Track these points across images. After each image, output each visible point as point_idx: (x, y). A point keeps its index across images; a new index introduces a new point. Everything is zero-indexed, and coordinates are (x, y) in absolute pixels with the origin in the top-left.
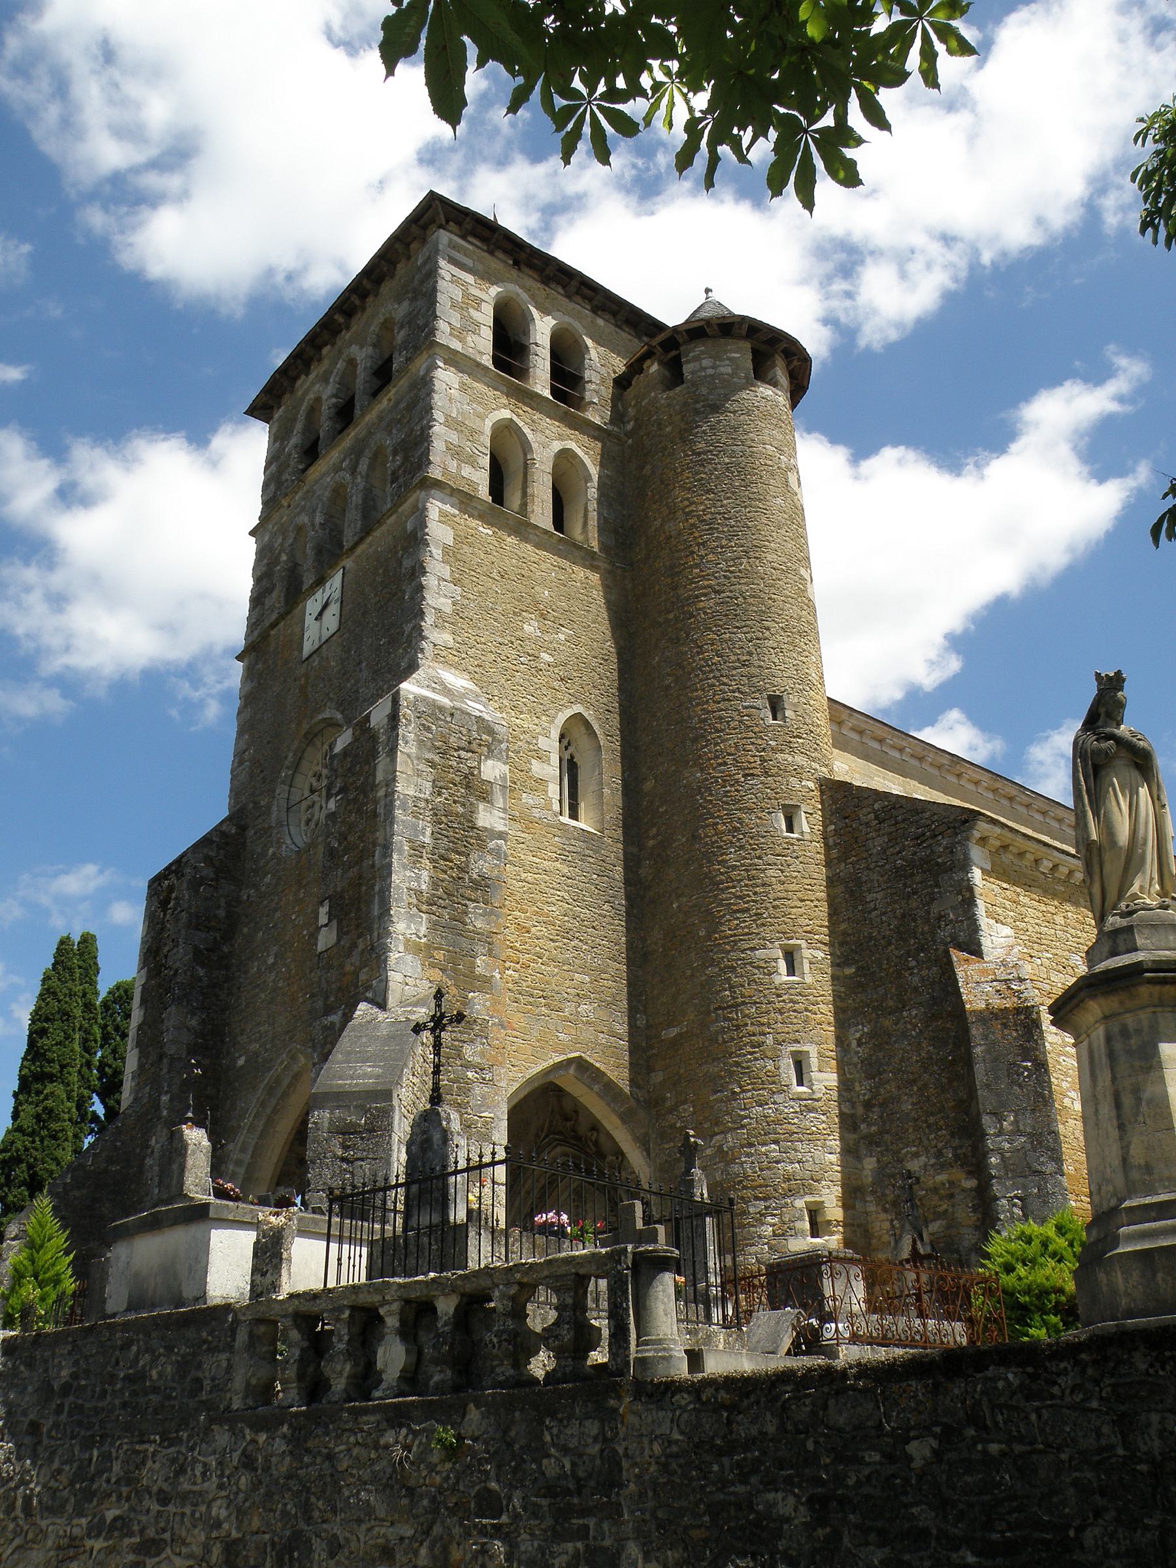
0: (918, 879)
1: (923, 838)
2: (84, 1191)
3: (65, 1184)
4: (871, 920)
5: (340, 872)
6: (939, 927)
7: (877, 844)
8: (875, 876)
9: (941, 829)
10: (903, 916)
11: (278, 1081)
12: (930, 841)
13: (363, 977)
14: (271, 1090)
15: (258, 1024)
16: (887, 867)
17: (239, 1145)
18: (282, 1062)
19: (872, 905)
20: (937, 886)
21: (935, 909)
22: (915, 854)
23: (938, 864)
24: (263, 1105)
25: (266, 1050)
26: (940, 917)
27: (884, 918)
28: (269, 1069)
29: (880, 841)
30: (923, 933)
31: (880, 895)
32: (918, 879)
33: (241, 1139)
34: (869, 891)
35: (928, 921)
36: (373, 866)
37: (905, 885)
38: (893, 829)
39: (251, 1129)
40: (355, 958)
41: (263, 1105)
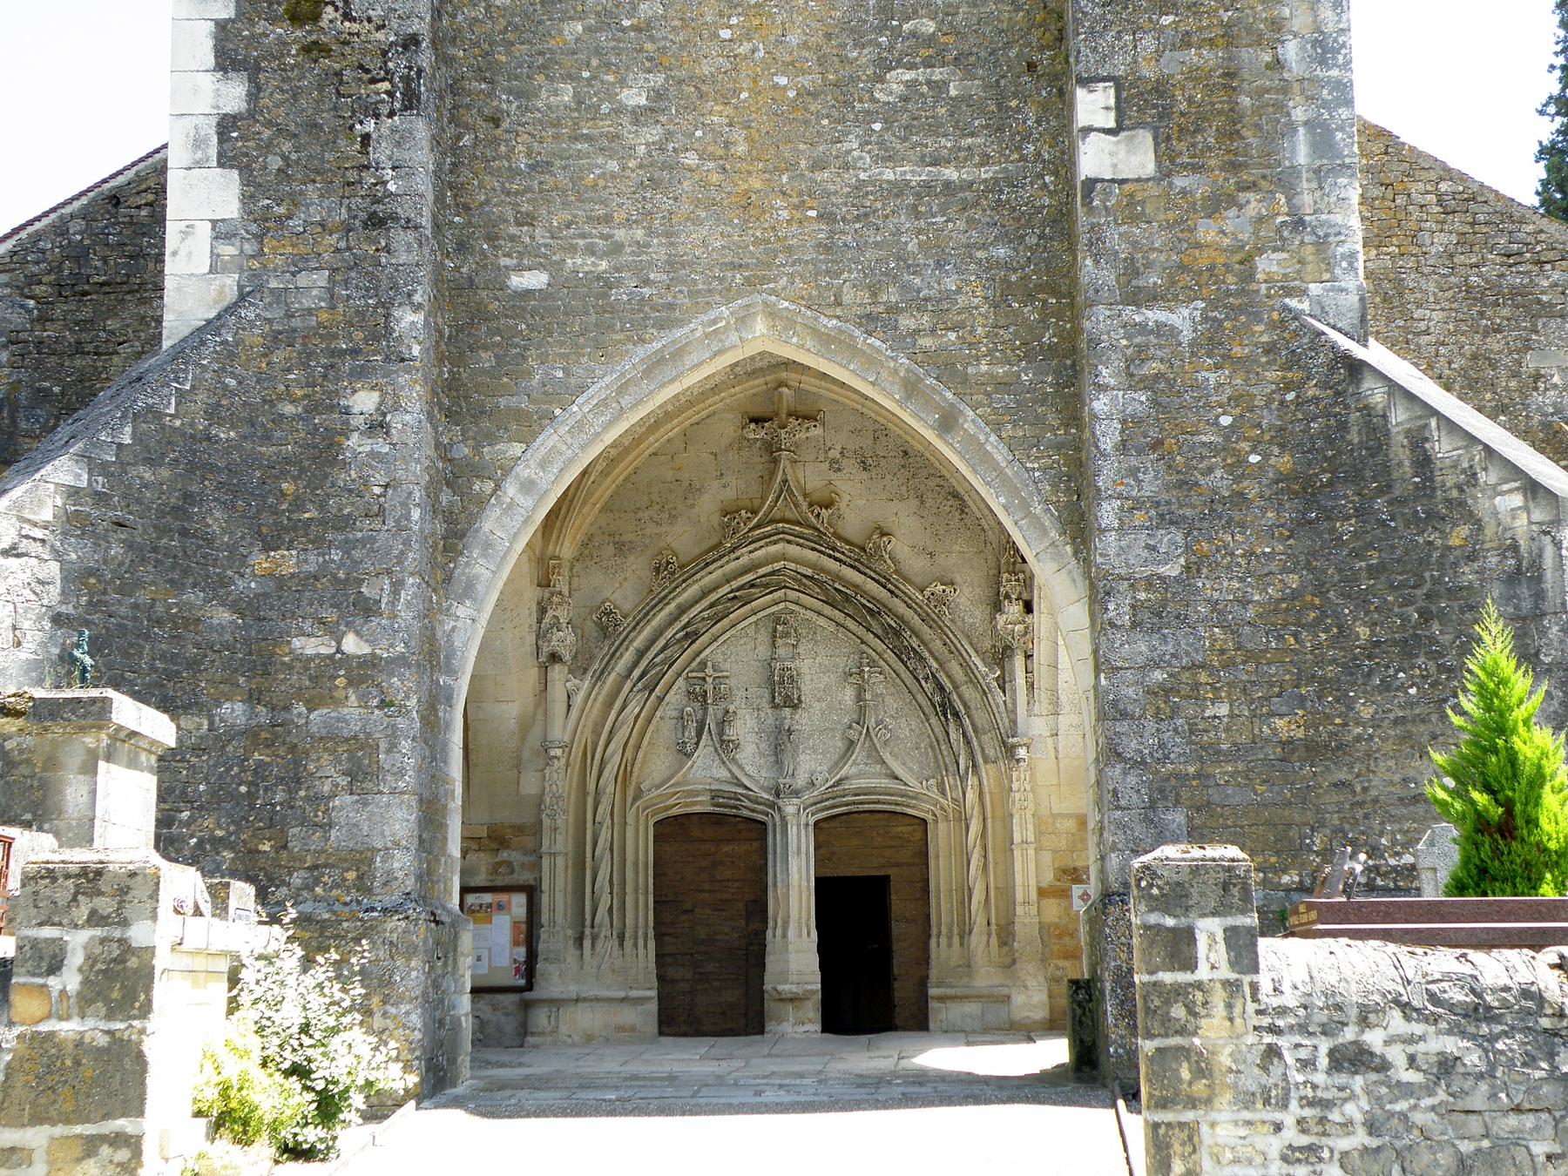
0: (1505, 312)
1: (1519, 259)
2: (165, 473)
3: (120, 445)
4: (1419, 346)
5: (1148, 42)
6: (1536, 389)
7: (1439, 242)
8: (1432, 287)
9: (1551, 255)
10: (1475, 357)
11: (678, 353)
12: (1530, 267)
13: (1269, 264)
14: (656, 364)
15: (607, 219)
16: (1452, 279)
17: (543, 451)
18: (714, 322)
19: (1422, 326)
20: (1537, 332)
21: (1531, 362)
22: (1502, 276)
23: (1539, 302)
24: (622, 389)
25: (647, 282)
26: (1537, 377)
27: (1442, 350)
28: (662, 325)
29: (1441, 238)
30: (1507, 389)
31: (1438, 316)
32: (1505, 312)
33: (548, 440)
34: (1419, 306)
35: (1515, 375)
36: (1277, 64)
37: (1482, 314)
38: (1468, 229)
39: (579, 426)
40: (1235, 225)
41: (622, 389)
